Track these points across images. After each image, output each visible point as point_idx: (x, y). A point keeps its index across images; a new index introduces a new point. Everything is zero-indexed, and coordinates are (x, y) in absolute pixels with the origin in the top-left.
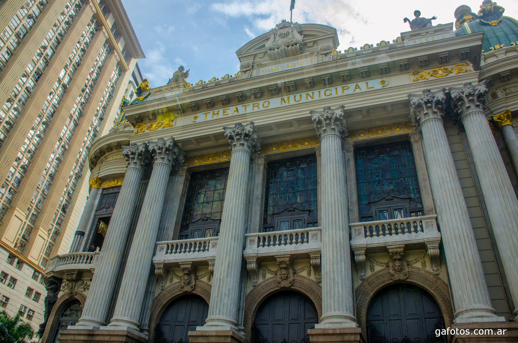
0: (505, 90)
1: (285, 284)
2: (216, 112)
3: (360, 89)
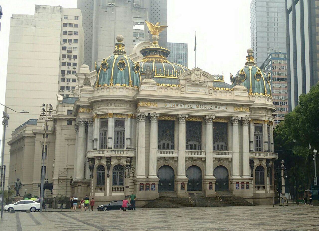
0: (254, 111)
1: (194, 164)
2: (174, 105)
3: (220, 109)
